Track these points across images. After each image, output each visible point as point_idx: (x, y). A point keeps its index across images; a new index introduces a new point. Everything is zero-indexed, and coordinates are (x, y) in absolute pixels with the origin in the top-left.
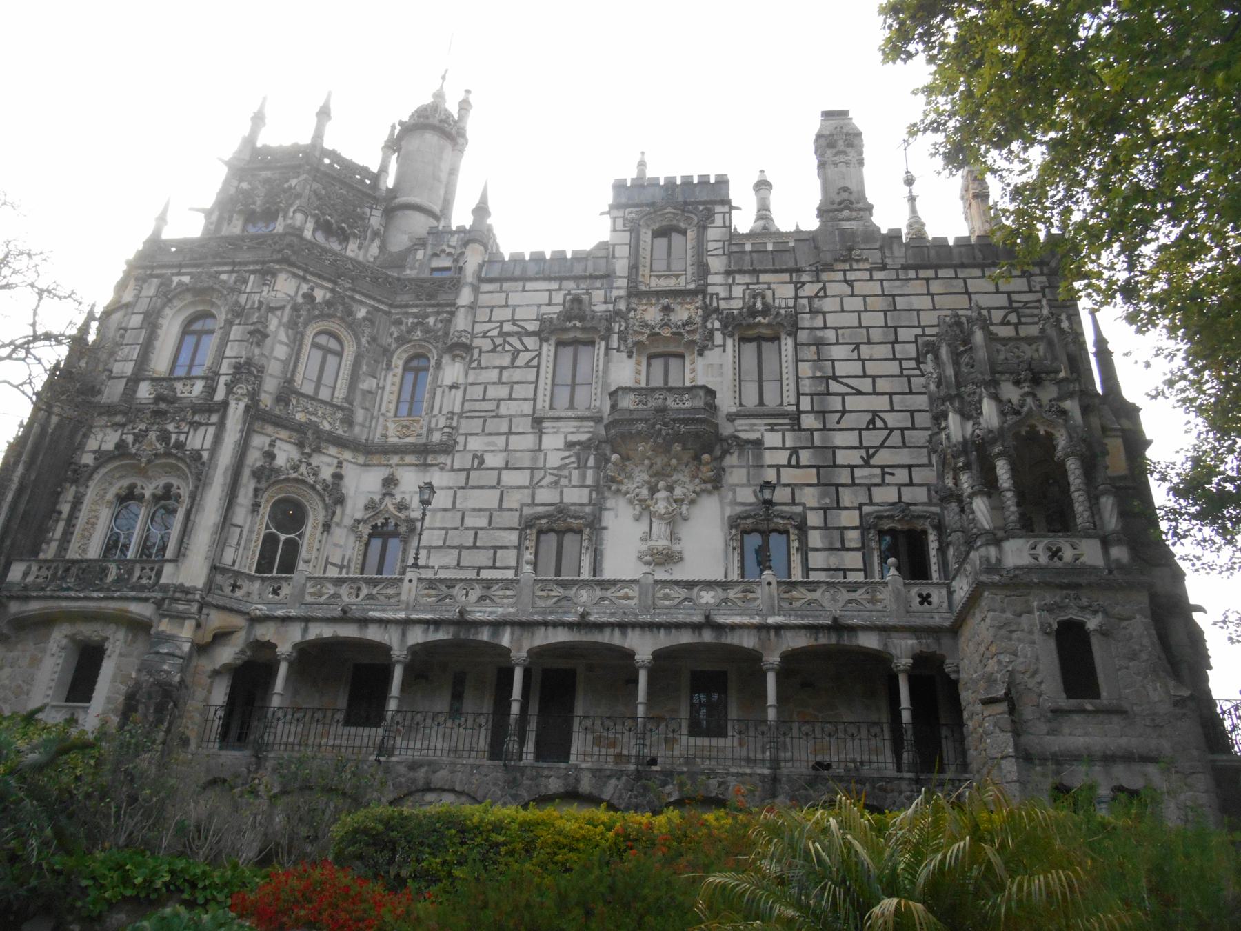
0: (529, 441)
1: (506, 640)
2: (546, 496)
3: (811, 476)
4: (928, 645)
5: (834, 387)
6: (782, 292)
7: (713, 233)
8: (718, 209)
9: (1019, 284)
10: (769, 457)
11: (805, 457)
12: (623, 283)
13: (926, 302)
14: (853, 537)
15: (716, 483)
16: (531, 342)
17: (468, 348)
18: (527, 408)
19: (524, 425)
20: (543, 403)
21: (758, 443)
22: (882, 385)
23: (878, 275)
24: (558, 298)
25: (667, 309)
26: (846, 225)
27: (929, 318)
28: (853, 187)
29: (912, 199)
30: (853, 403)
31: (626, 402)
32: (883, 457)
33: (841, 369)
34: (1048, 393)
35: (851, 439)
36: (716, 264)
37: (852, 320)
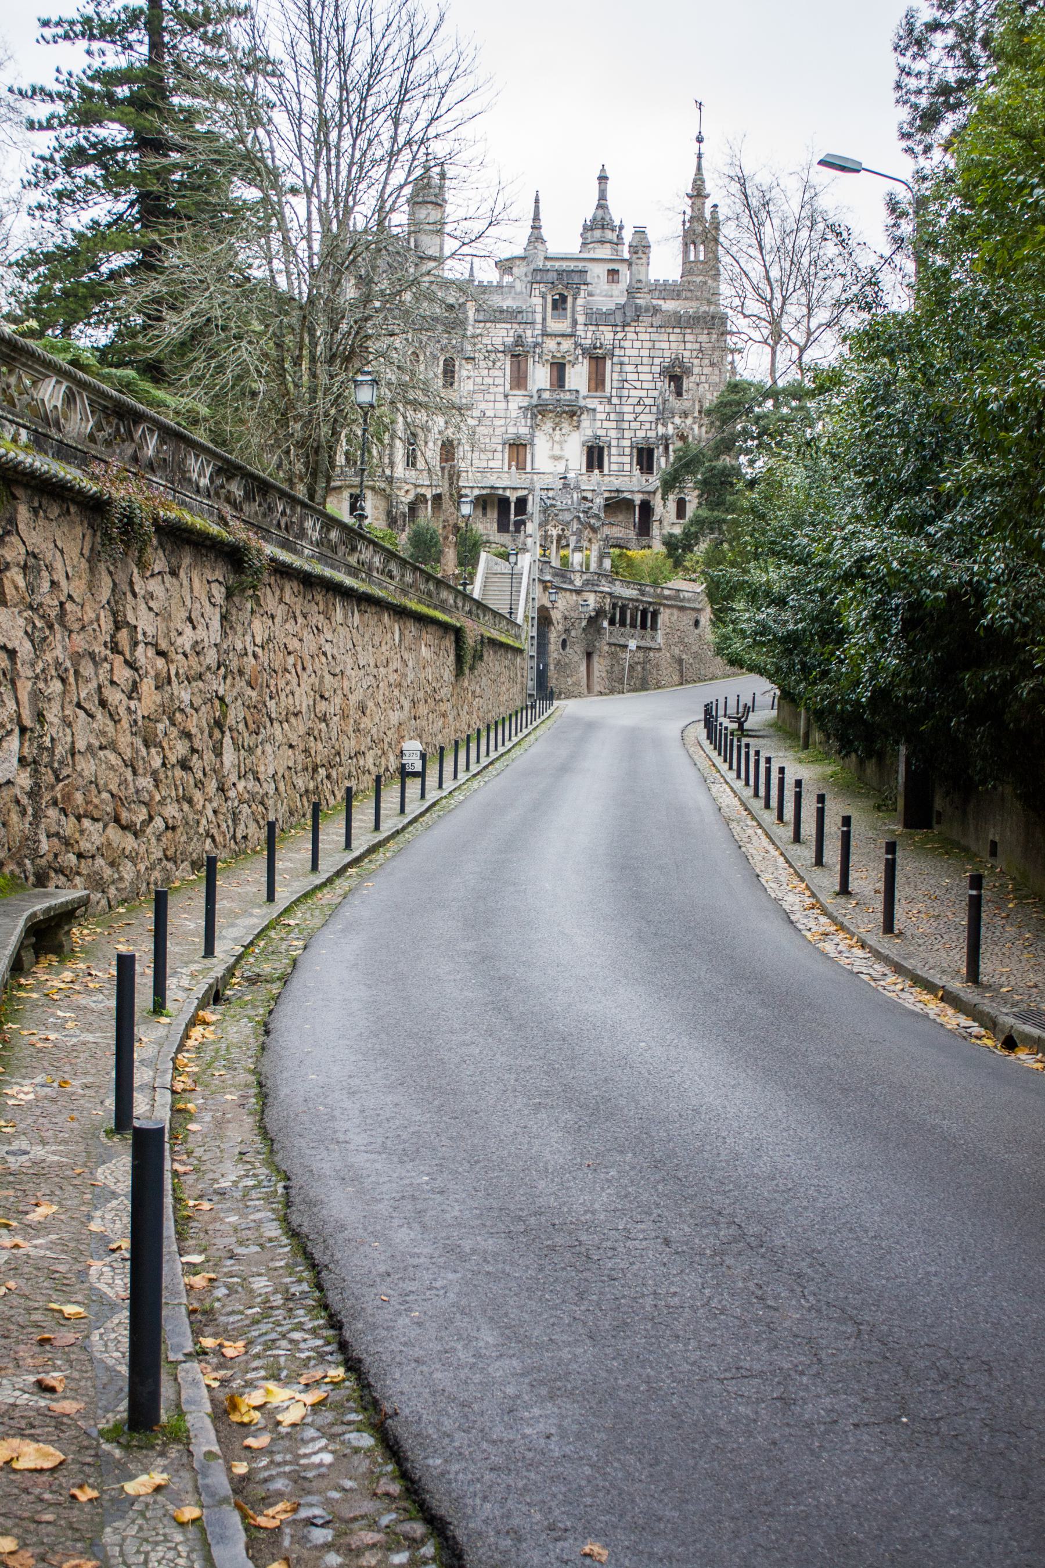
0: (502, 405)
1: (508, 493)
2: (512, 430)
3: (614, 425)
4: (646, 497)
5: (626, 385)
6: (607, 335)
7: (580, 301)
8: (583, 287)
9: (703, 338)
10: (599, 416)
11: (613, 416)
12: (539, 326)
13: (665, 345)
14: (627, 451)
15: (578, 427)
16: (500, 355)
17: (473, 359)
18: (501, 389)
19: (500, 397)
20: (508, 386)
21: (594, 410)
22: (645, 385)
23: (650, 330)
24: (511, 333)
25: (559, 344)
26: (638, 301)
27: (667, 354)
28: (644, 279)
29: (700, 156)
30: (633, 393)
31: (546, 395)
32: (641, 418)
33: (630, 377)
34: (689, 421)
35: (630, 409)
36: (581, 319)
37: (635, 352)
